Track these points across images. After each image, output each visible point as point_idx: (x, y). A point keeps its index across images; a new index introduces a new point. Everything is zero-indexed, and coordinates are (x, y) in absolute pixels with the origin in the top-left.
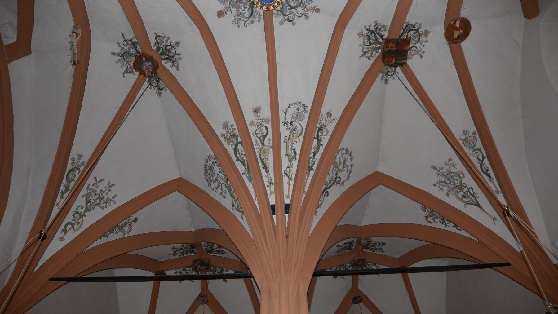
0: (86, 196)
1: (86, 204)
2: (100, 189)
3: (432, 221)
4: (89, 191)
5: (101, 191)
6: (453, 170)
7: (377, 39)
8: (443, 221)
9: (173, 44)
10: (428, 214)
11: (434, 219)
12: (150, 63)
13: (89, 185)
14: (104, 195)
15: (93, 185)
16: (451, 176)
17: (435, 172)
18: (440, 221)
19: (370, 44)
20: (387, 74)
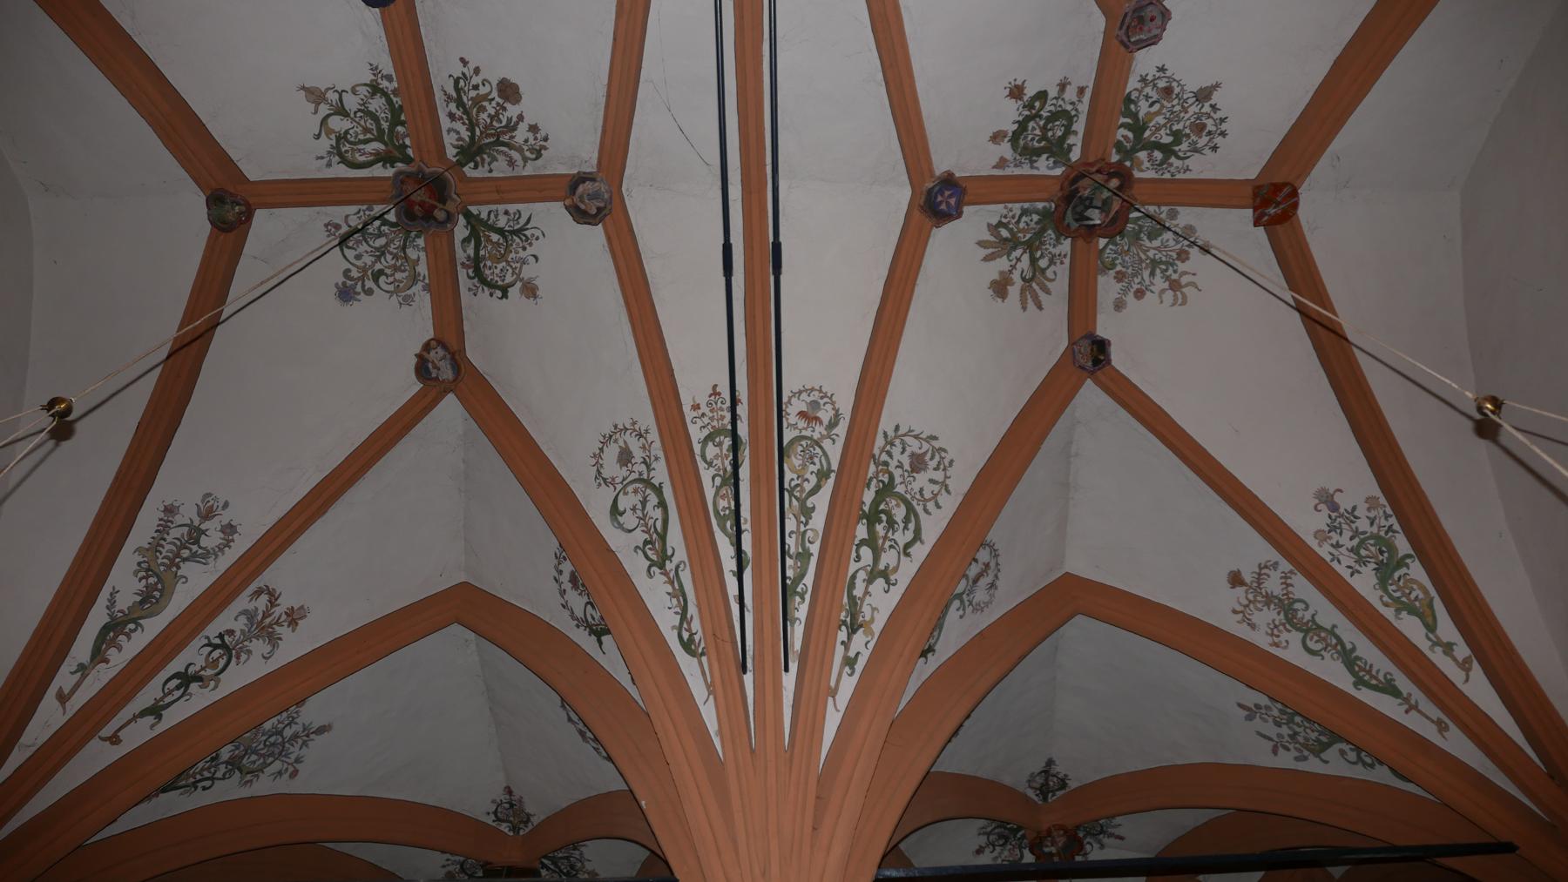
0: (1317, 754)
1: (1329, 745)
2: (1278, 730)
3: (251, 607)
4: (1306, 753)
5: (1278, 725)
6: (277, 766)
7: (555, 863)
8: (223, 646)
9: (987, 851)
10: (277, 611)
11: (250, 615)
12: (1046, 850)
13: (1297, 759)
14: (1275, 713)
15: (1288, 749)
16: (272, 754)
17: (315, 726)
18: (231, 632)
19: (567, 858)
20: (512, 805)
